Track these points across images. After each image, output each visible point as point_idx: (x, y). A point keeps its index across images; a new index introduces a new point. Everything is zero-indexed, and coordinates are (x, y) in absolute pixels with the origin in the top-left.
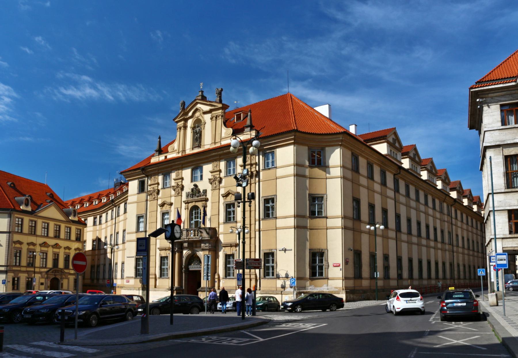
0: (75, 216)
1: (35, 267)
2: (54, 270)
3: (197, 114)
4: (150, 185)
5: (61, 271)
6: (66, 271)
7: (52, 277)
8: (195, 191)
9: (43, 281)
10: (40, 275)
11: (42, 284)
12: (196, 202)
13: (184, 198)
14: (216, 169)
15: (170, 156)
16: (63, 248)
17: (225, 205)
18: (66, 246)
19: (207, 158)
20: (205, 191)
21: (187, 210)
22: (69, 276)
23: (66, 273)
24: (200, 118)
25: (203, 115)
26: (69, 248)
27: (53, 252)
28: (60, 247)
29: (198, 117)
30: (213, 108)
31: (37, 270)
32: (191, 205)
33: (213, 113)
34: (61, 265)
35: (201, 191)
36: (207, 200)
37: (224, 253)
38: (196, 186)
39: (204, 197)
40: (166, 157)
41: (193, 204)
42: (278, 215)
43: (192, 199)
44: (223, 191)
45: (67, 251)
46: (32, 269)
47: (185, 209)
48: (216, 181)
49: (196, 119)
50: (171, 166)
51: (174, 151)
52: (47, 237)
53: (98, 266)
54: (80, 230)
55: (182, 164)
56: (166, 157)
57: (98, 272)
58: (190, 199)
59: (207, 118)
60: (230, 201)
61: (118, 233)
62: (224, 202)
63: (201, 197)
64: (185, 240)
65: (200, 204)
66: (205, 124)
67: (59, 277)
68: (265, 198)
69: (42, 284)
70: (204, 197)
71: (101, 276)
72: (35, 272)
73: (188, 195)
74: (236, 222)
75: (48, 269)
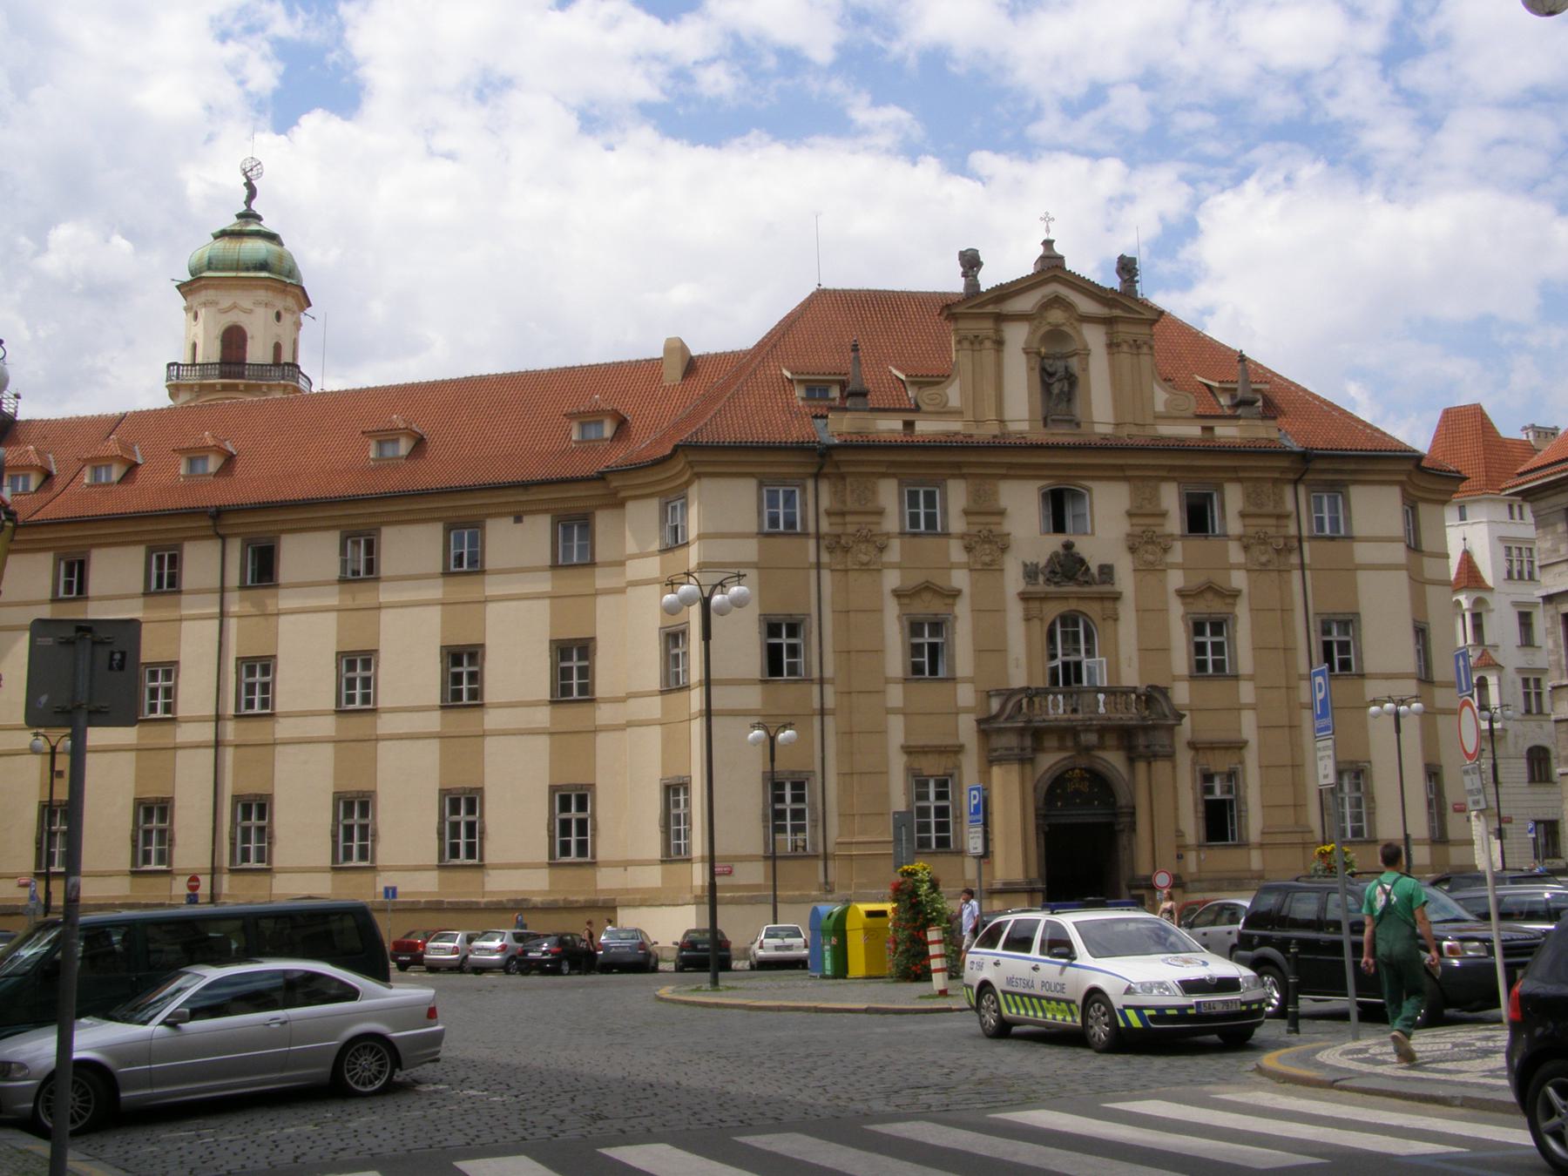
3: (1056, 316)
4: (829, 514)
8: (1068, 567)
12: (1080, 599)
13: (1014, 581)
14: (1148, 508)
15: (926, 427)
17: (1190, 624)
19: (1121, 467)
20: (1107, 571)
21: (1036, 623)
24: (1066, 329)
25: (1076, 324)
29: (1057, 325)
30: (1117, 312)
32: (1053, 610)
33: (1122, 328)
35: (1094, 570)
36: (1116, 597)
37: (1198, 768)
38: (1068, 546)
39: (1106, 588)
40: (909, 425)
41: (1073, 605)
42: (1370, 666)
43: (1052, 588)
44: (1176, 579)
47: (1028, 619)
48: (1147, 543)
49: (1048, 328)
50: (958, 465)
51: (944, 412)
55: (1011, 466)
56: (909, 425)
58: (1041, 586)
59: (1094, 337)
60: (1210, 614)
62: (1188, 613)
63: (1095, 588)
64: (1095, 722)
65: (1093, 609)
66: (1088, 354)
68: (1325, 617)
70: (1106, 588)
73: (1031, 573)
74: (1236, 677)
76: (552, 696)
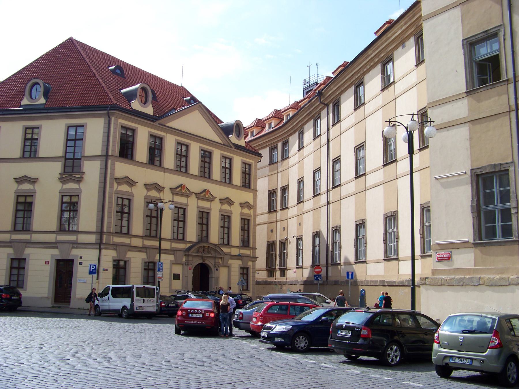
0: (238, 136)
1: (160, 239)
2: (201, 247)
5: (215, 251)
6: (225, 250)
7: (198, 261)
9: (178, 270)
10: (171, 257)
11: (176, 277)
16: (217, 200)
18: (223, 196)
22: (231, 262)
23: (225, 254)
26: (228, 201)
27: (198, 207)
28: (211, 199)
31: (165, 245)
34: (214, 237)
45: (226, 207)
46: (156, 243)
52: (184, 174)
53: (284, 244)
54: (250, 165)
57: (283, 256)
61: (337, 160)
67: (210, 262)
69: (176, 277)
71: (291, 261)
72: (160, 251)
75: (188, 245)
76: (420, 147)
